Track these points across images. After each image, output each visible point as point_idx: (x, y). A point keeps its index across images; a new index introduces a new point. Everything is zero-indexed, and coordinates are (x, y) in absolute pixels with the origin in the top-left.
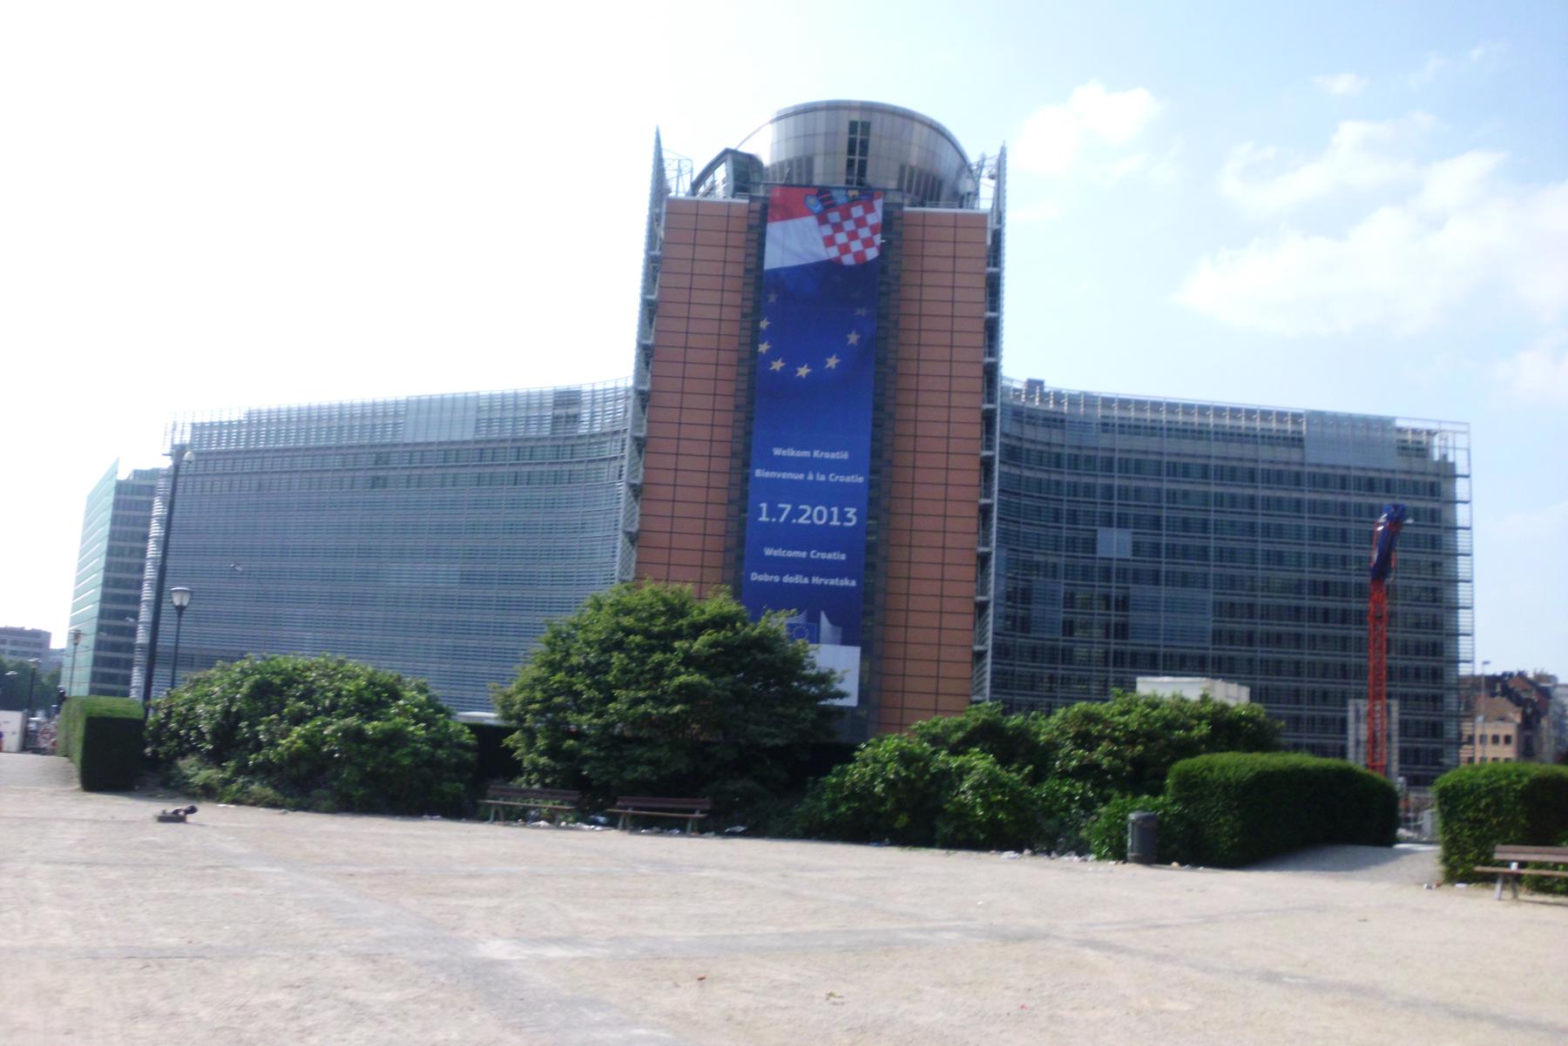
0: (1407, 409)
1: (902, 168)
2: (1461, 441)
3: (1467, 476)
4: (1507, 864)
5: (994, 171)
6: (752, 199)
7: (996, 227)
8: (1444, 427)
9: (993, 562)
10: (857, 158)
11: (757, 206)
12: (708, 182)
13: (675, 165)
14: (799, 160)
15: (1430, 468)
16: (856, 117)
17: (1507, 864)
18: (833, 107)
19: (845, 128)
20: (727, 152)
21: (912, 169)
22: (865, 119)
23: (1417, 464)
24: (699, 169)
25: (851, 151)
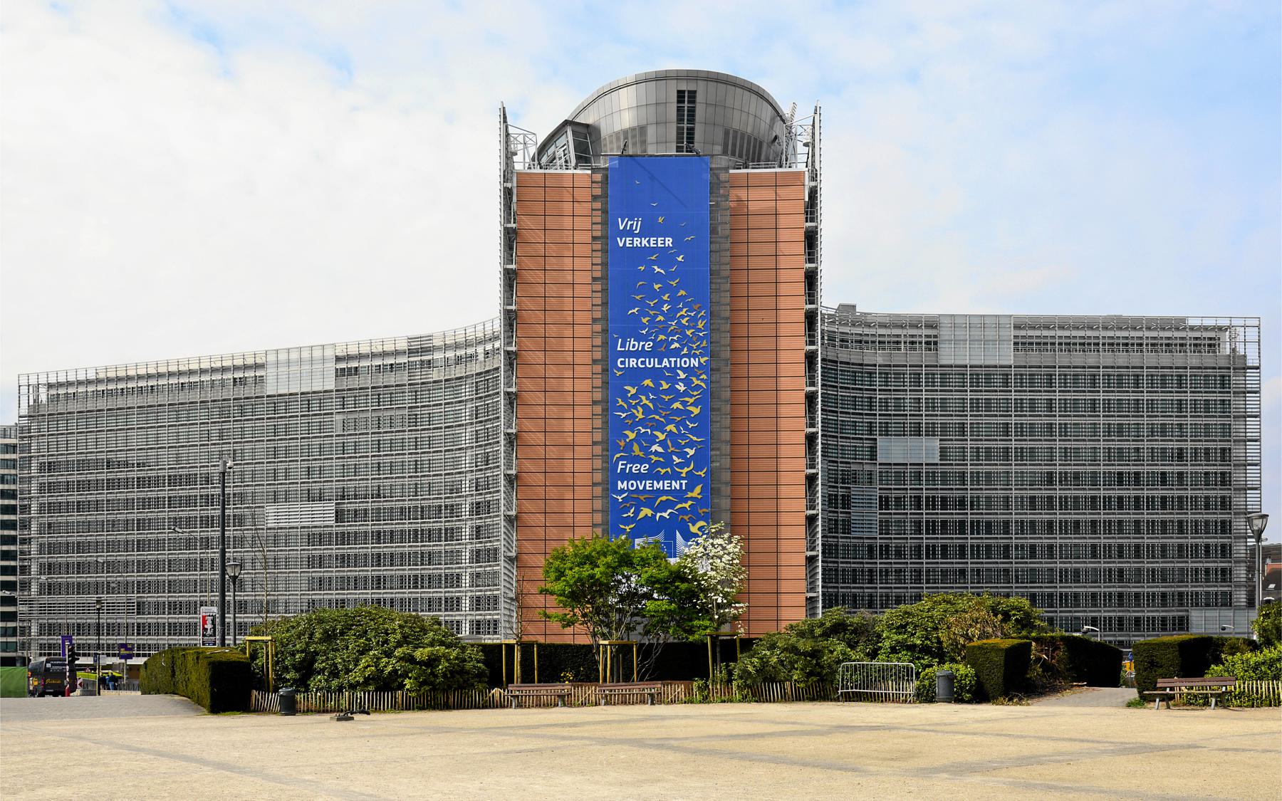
0: (1196, 307)
1: (727, 133)
2: (1252, 334)
3: (1258, 368)
4: (1165, 689)
5: (809, 140)
6: (594, 170)
7: (813, 184)
8: (1234, 323)
9: (820, 523)
10: (685, 126)
11: (598, 177)
12: (550, 151)
13: (521, 139)
14: (633, 129)
15: (1223, 363)
16: (683, 87)
17: (1165, 689)
18: (662, 78)
19: (674, 98)
20: (566, 123)
21: (736, 132)
22: (692, 88)
23: (1208, 359)
24: (541, 138)
25: (680, 120)
